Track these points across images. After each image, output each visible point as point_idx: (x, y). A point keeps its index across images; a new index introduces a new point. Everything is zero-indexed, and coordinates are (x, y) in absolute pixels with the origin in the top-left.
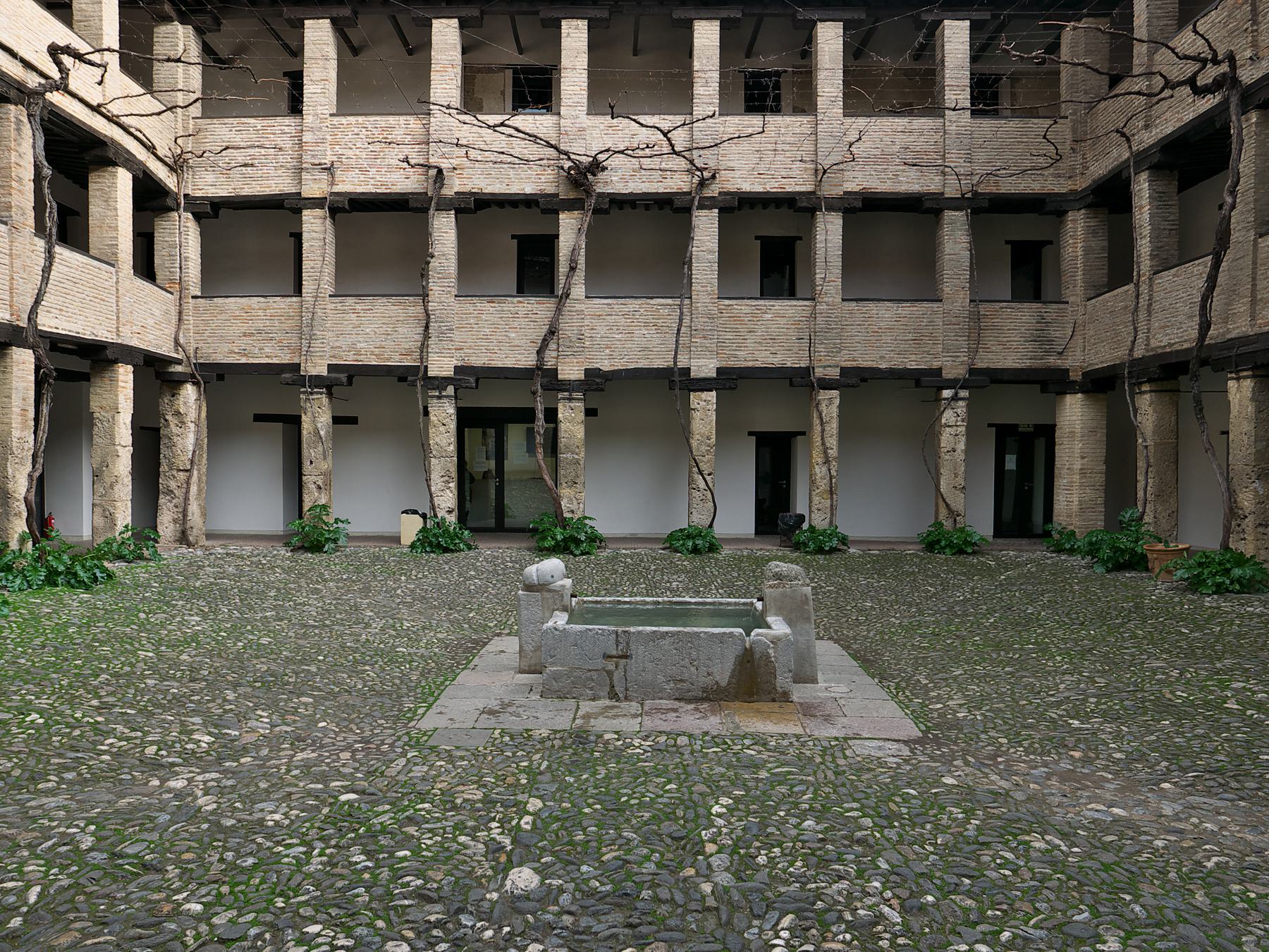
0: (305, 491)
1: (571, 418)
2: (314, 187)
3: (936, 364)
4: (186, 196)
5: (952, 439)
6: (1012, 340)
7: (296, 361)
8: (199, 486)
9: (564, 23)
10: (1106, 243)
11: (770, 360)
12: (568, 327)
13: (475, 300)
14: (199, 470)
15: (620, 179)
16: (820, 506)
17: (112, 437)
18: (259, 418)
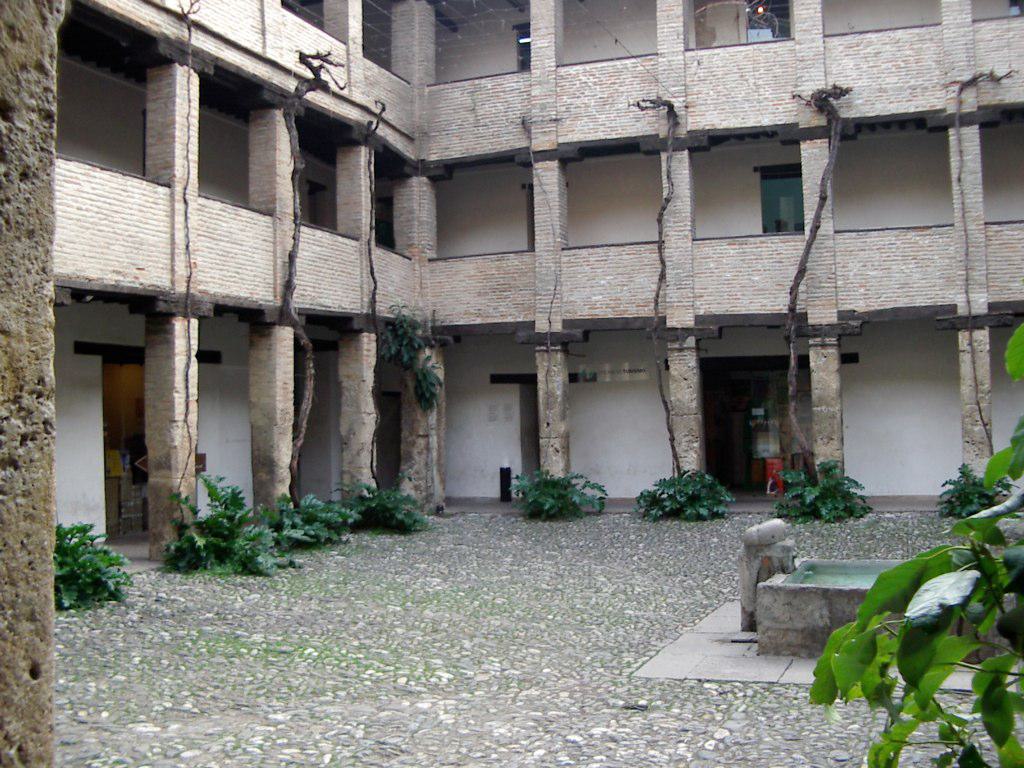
1: (824, 367)
2: (542, 142)
12: (818, 268)
15: (866, 104)
17: (358, 407)
18: (497, 379)
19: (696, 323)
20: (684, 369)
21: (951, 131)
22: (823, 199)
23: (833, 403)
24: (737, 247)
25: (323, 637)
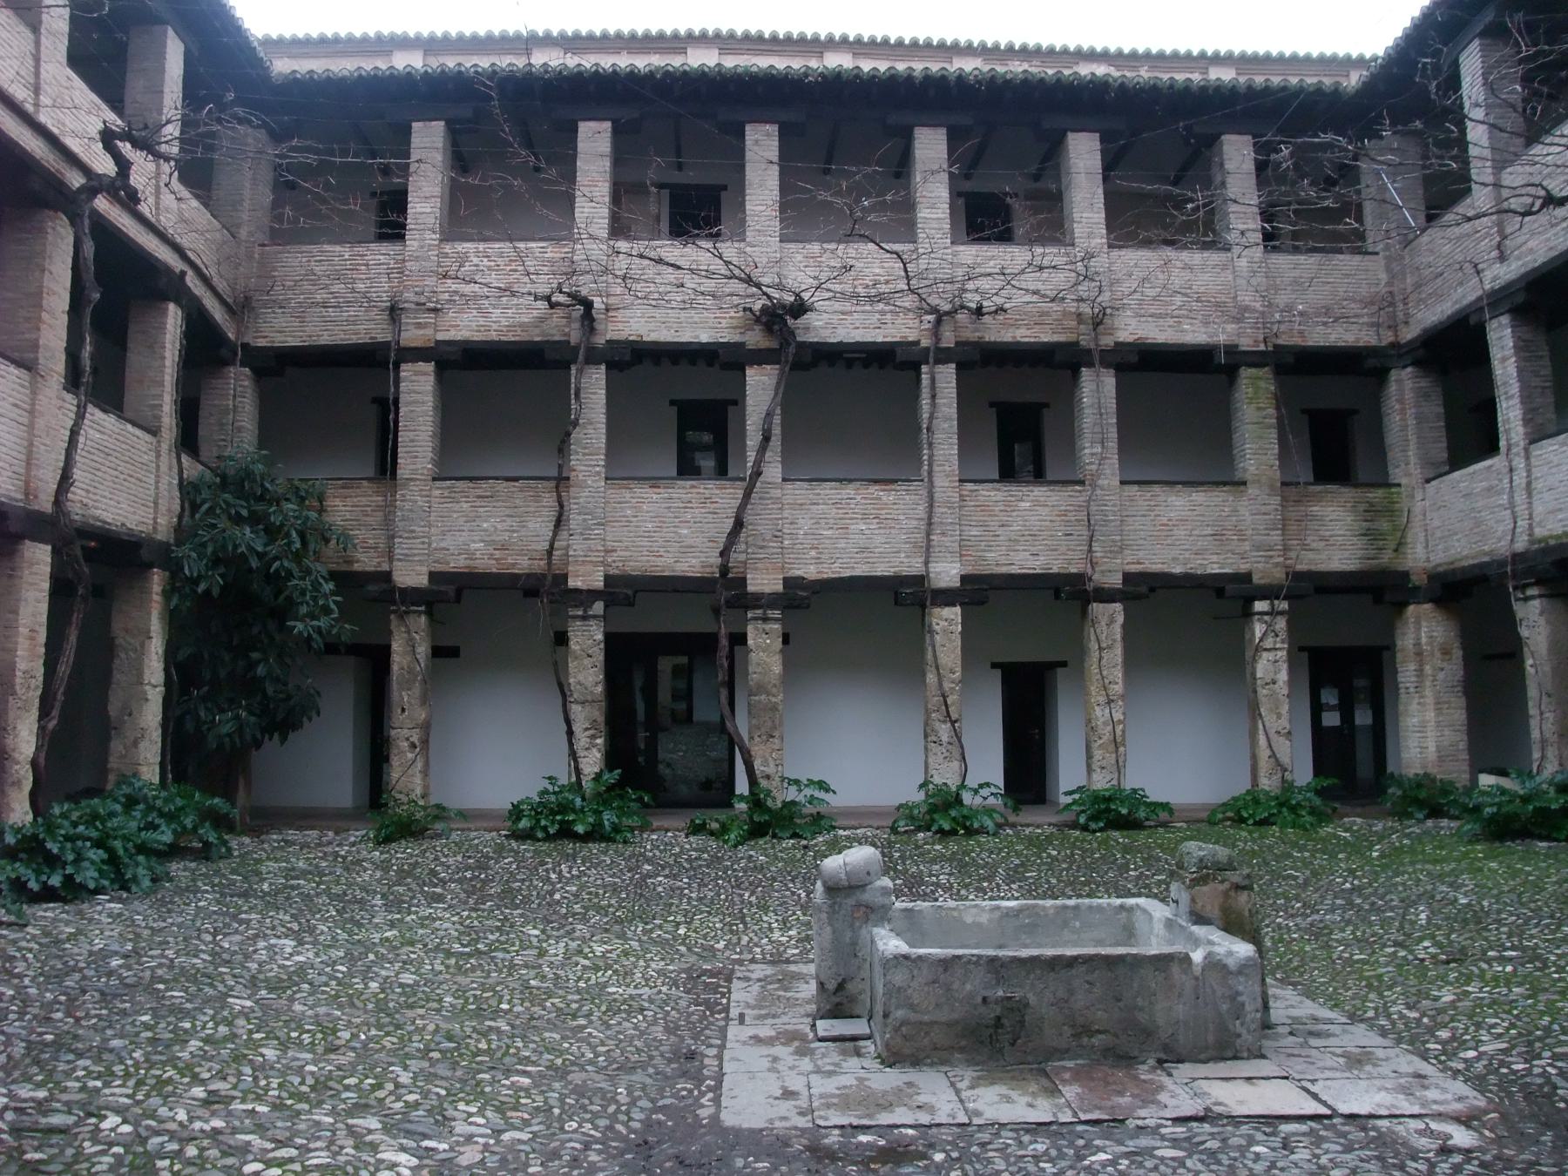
0: (394, 751)
1: (764, 646)
2: (413, 335)
3: (1244, 567)
4: (245, 346)
5: (1271, 668)
6: (1334, 537)
7: (385, 567)
9: (748, 128)
10: (1441, 410)
11: (1030, 564)
12: (760, 521)
13: (632, 484)
15: (834, 323)
16: (1104, 763)
17: (140, 674)
20: (587, 641)
21: (924, 368)
22: (766, 438)
23: (774, 690)
25: (131, 1083)
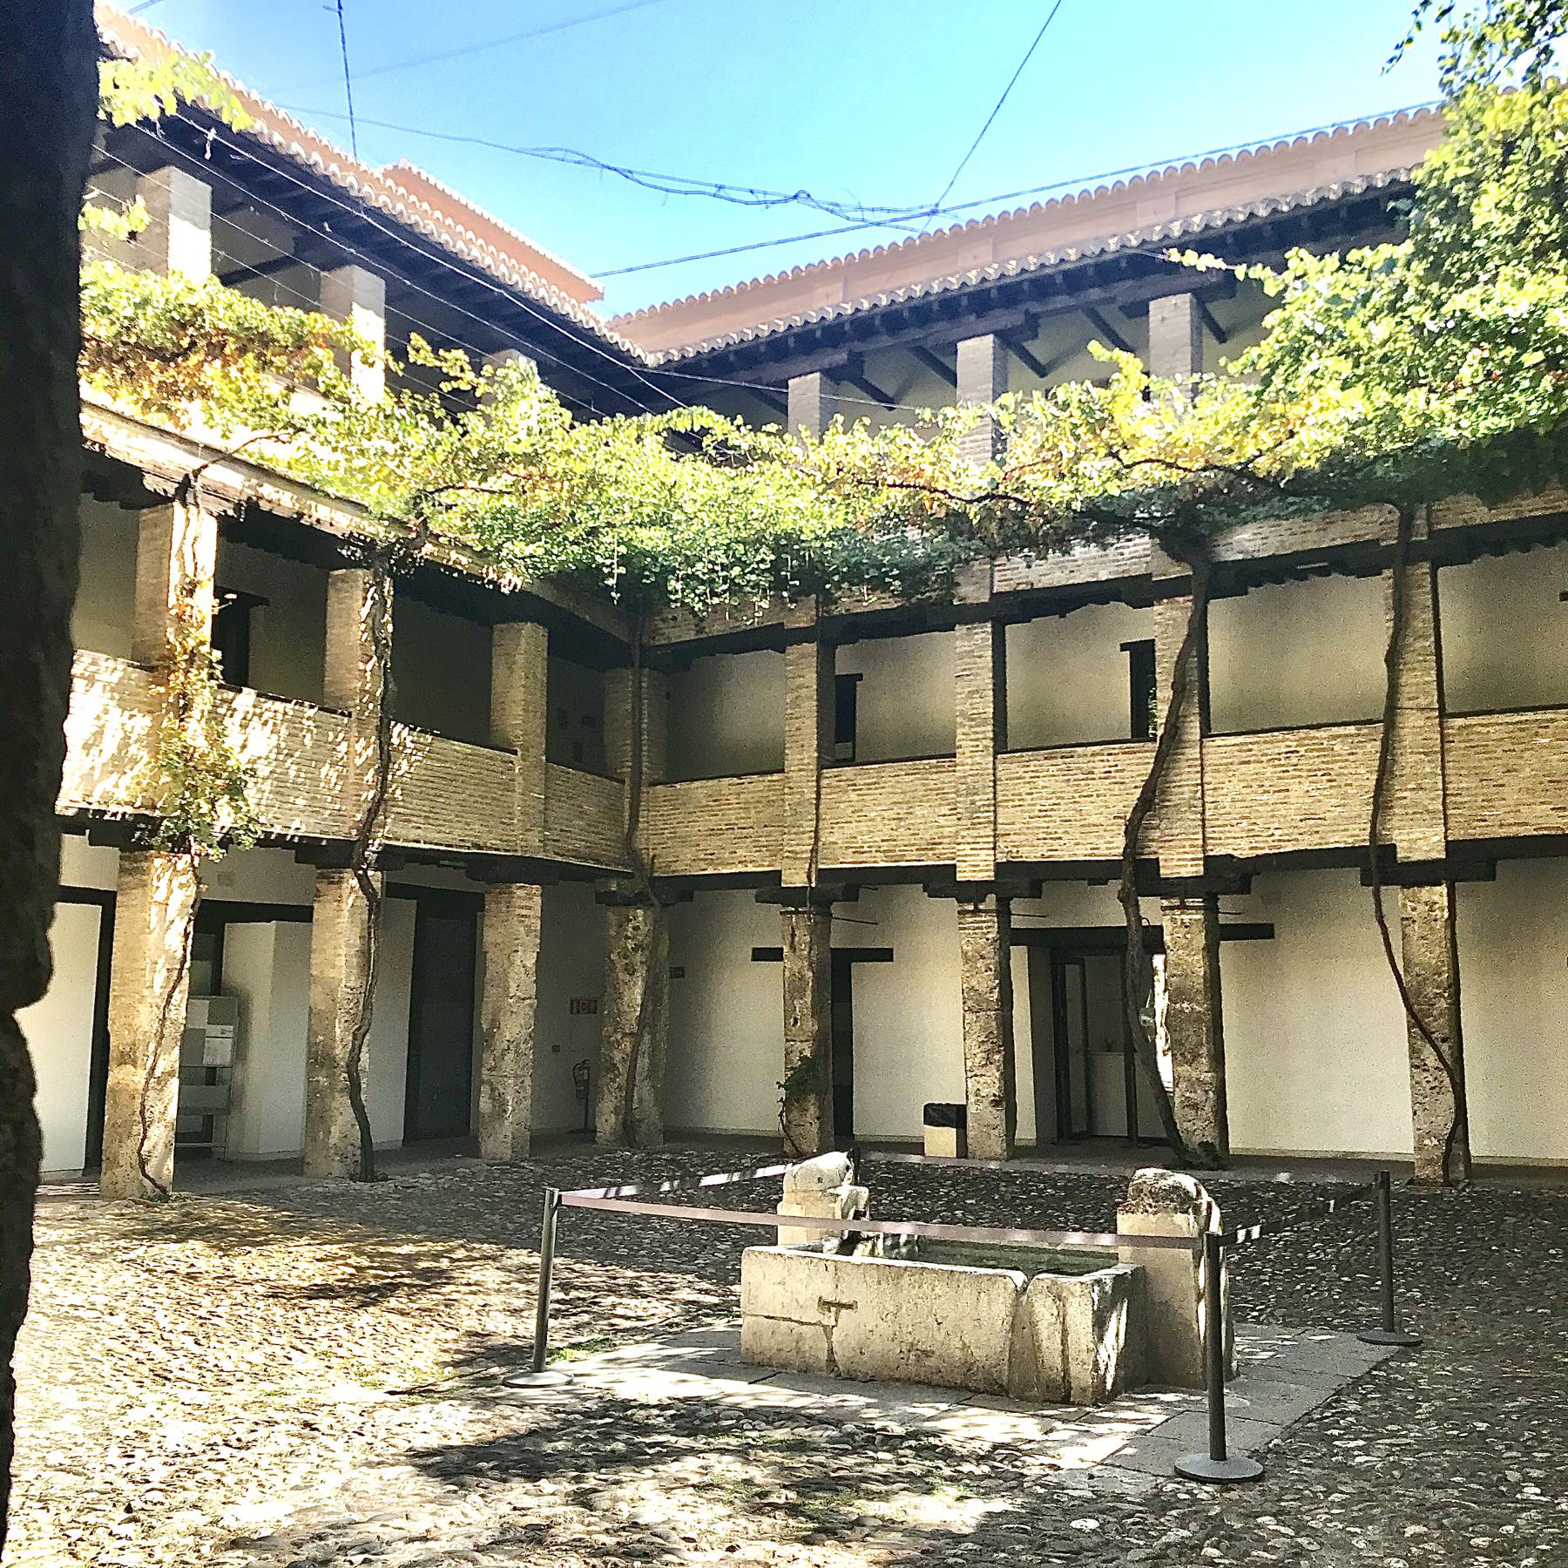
8: (652, 1056)
14: (653, 1035)
19: (996, 876)
24: (1060, 761)
